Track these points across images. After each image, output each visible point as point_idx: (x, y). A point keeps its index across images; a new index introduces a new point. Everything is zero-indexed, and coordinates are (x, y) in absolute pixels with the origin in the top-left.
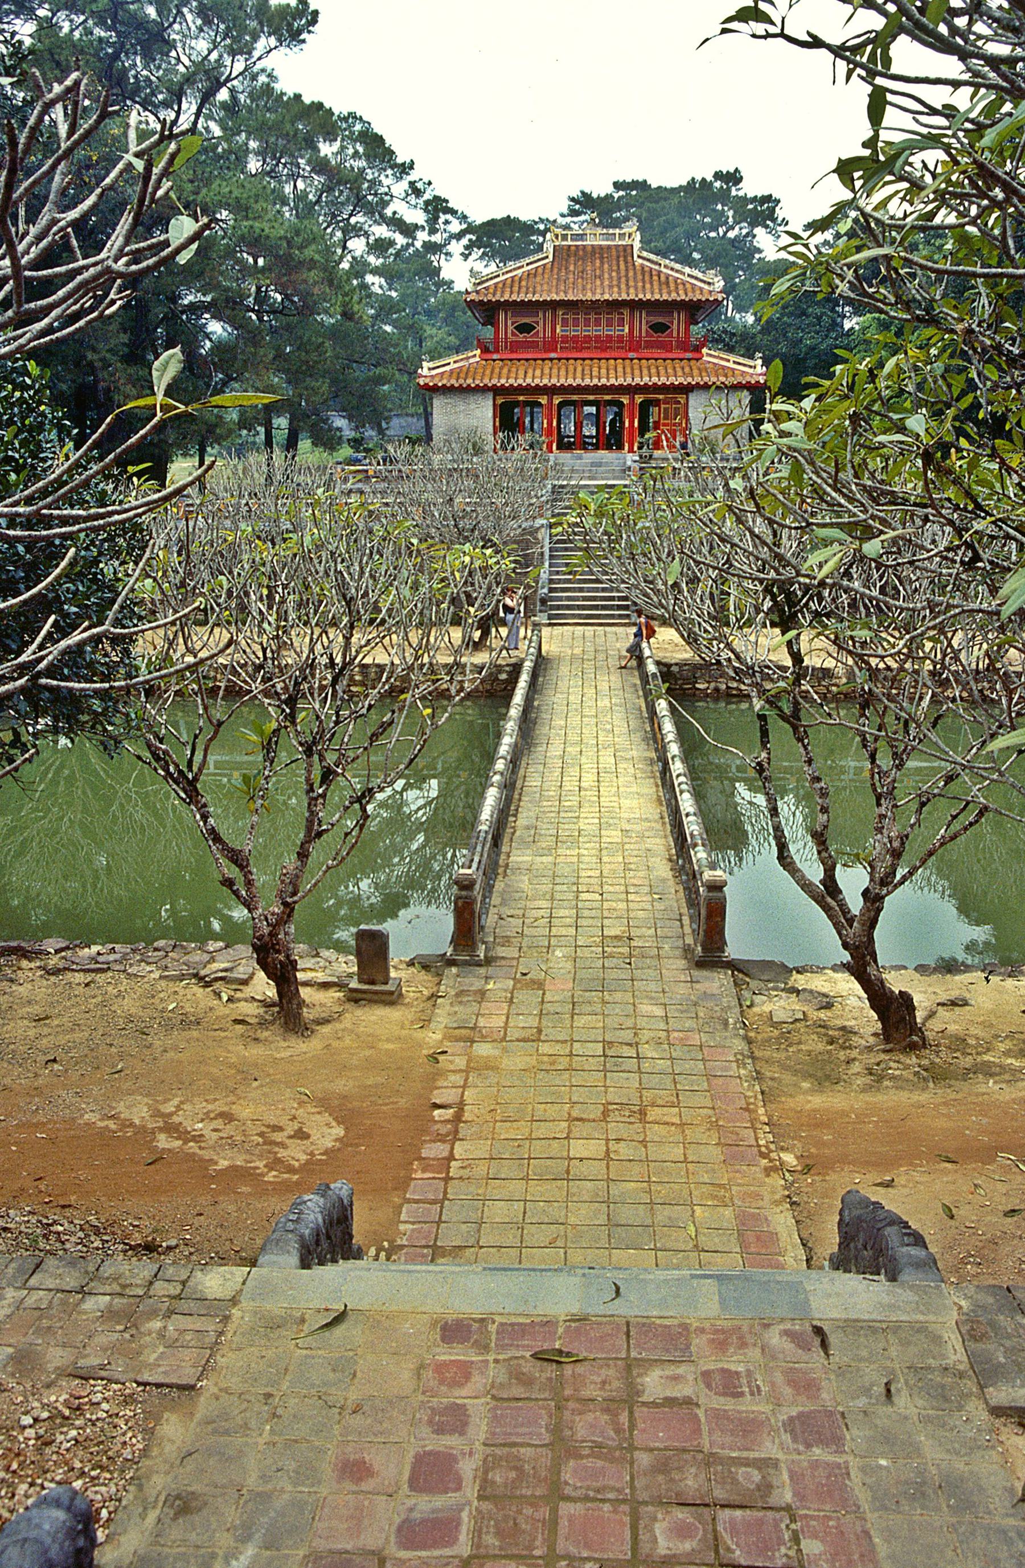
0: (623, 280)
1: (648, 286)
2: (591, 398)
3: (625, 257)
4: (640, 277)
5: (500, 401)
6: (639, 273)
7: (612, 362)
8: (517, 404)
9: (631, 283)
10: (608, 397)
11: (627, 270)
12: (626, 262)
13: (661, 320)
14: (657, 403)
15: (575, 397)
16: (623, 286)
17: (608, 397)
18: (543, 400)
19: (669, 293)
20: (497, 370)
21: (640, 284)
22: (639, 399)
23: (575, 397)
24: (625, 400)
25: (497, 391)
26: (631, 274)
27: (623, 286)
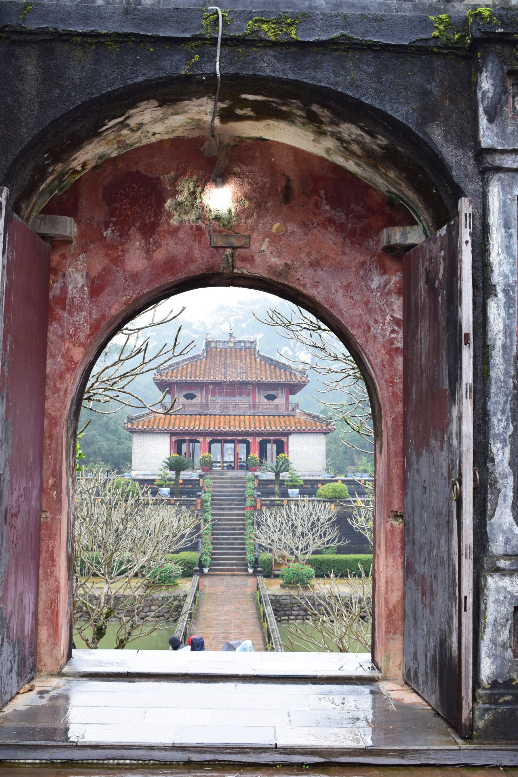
0: (249, 369)
1: (263, 373)
2: (230, 438)
3: (250, 356)
4: (259, 368)
5: (174, 439)
6: (258, 365)
7: (242, 417)
8: (184, 441)
9: (254, 371)
10: (240, 438)
11: (251, 363)
12: (251, 359)
13: (272, 393)
14: (269, 441)
15: (219, 438)
16: (249, 373)
17: (240, 438)
18: (200, 439)
19: (276, 377)
20: (172, 421)
21: (259, 372)
22: (258, 439)
23: (219, 438)
24: (250, 439)
25: (172, 434)
26: (254, 366)
27: (249, 373)
